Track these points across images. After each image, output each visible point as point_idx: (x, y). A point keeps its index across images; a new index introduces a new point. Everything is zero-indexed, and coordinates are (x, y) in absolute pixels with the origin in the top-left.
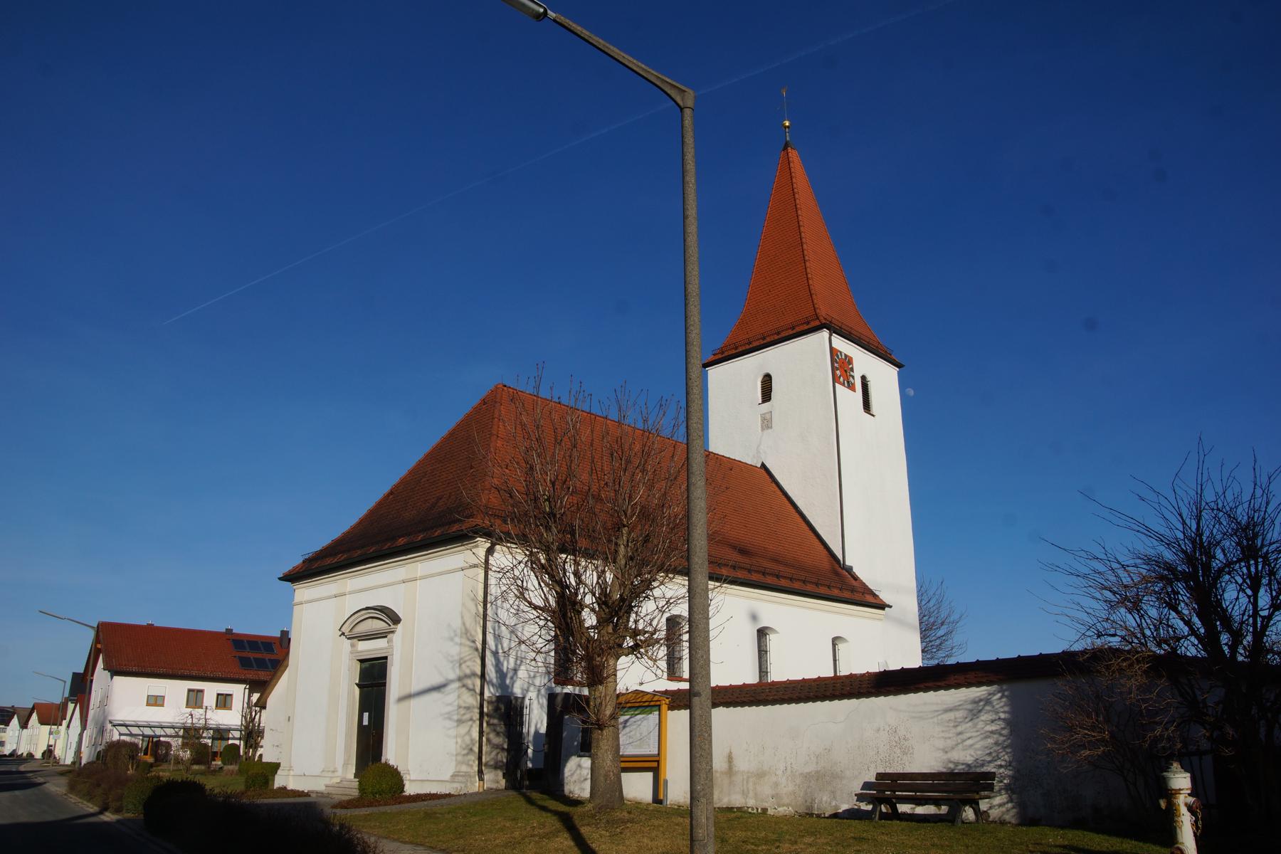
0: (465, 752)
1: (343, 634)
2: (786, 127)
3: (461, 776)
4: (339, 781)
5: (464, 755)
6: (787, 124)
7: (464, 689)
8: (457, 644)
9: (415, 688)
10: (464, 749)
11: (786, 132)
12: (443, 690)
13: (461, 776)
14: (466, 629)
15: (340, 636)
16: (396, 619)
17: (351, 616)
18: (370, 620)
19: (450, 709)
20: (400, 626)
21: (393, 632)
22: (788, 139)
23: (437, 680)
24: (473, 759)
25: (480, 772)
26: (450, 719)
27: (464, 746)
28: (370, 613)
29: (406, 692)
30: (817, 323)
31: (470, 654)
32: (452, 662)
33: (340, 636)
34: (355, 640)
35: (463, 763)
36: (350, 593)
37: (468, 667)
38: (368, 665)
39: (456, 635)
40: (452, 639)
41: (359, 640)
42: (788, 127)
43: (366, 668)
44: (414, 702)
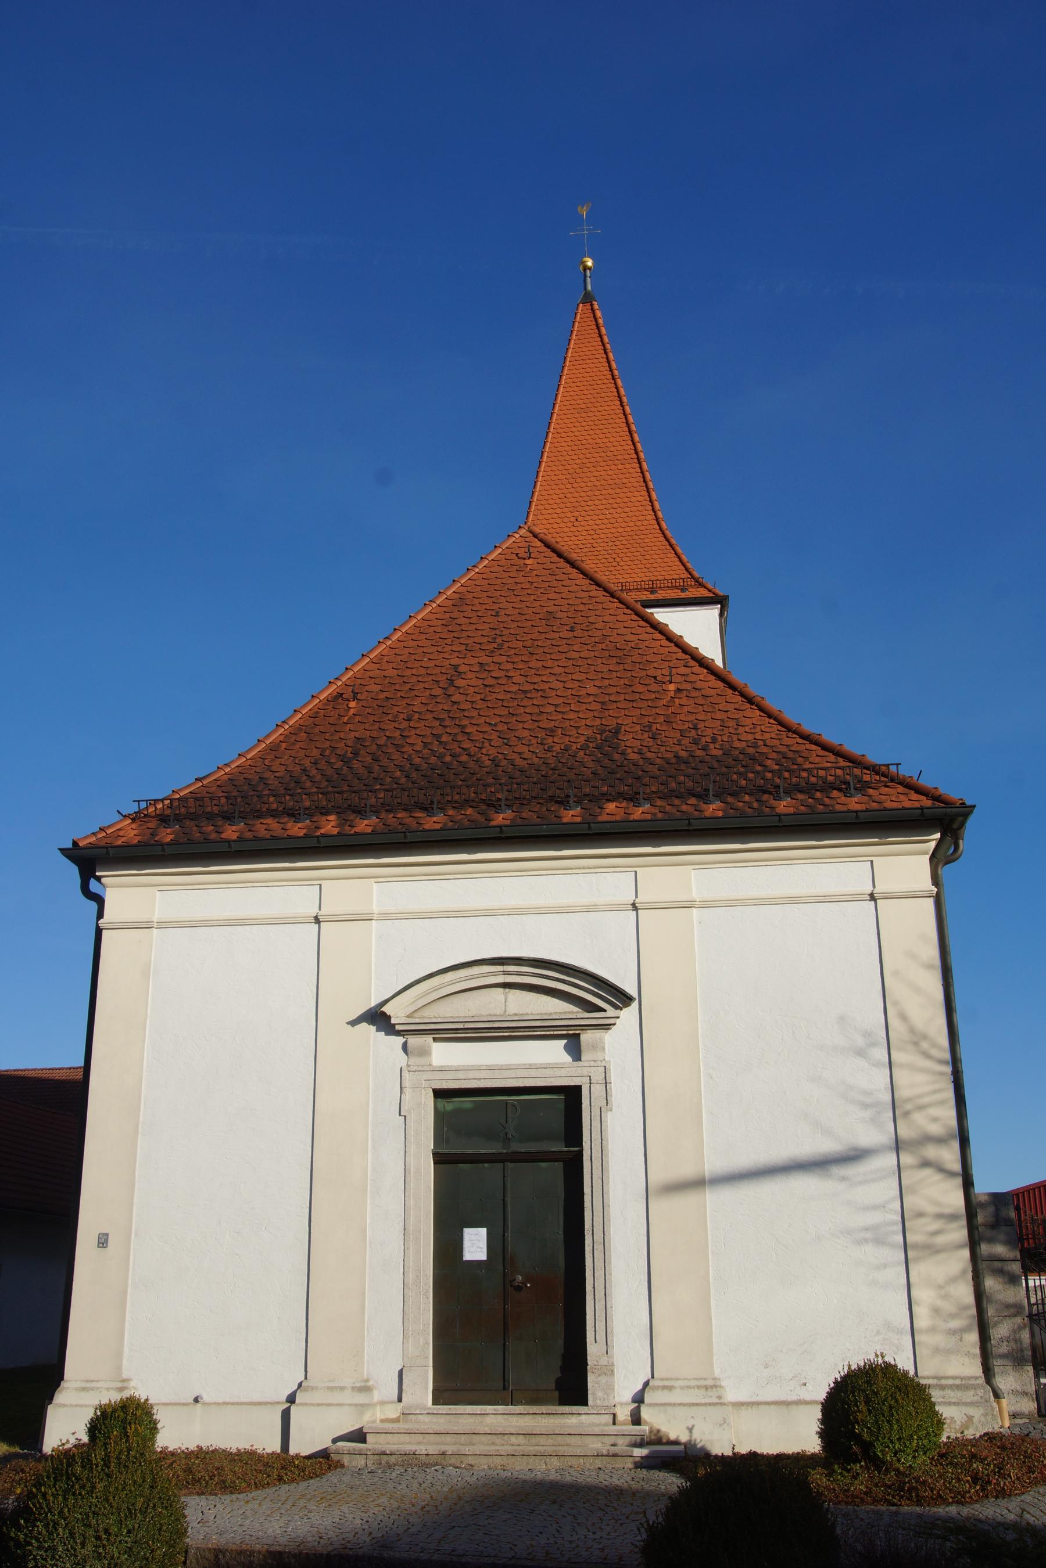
0: (955, 1324)
1: (378, 1018)
2: (586, 268)
3: (958, 1387)
4: (393, 1415)
5: (953, 1332)
6: (590, 263)
7: (927, 1172)
8: (877, 1064)
9: (713, 1164)
10: (953, 1316)
11: (585, 276)
12: (837, 1171)
13: (958, 1387)
14: (912, 1030)
15: (353, 1023)
16: (623, 999)
17: (431, 976)
18: (501, 990)
19: (875, 1218)
20: (628, 1016)
21: (607, 1027)
22: (589, 288)
23: (827, 1146)
24: (974, 1337)
25: (988, 1372)
26: (879, 1241)
27: (948, 1307)
28: (505, 973)
29: (687, 1171)
30: (702, 593)
31: (935, 1092)
32: (865, 1106)
33: (353, 1023)
34: (429, 1039)
35: (949, 1352)
36: (386, 917)
37: (935, 1120)
38: (468, 1106)
39: (873, 1044)
40: (860, 1053)
41: (435, 1039)
42: (590, 269)
43: (457, 1112)
44: (713, 1199)
